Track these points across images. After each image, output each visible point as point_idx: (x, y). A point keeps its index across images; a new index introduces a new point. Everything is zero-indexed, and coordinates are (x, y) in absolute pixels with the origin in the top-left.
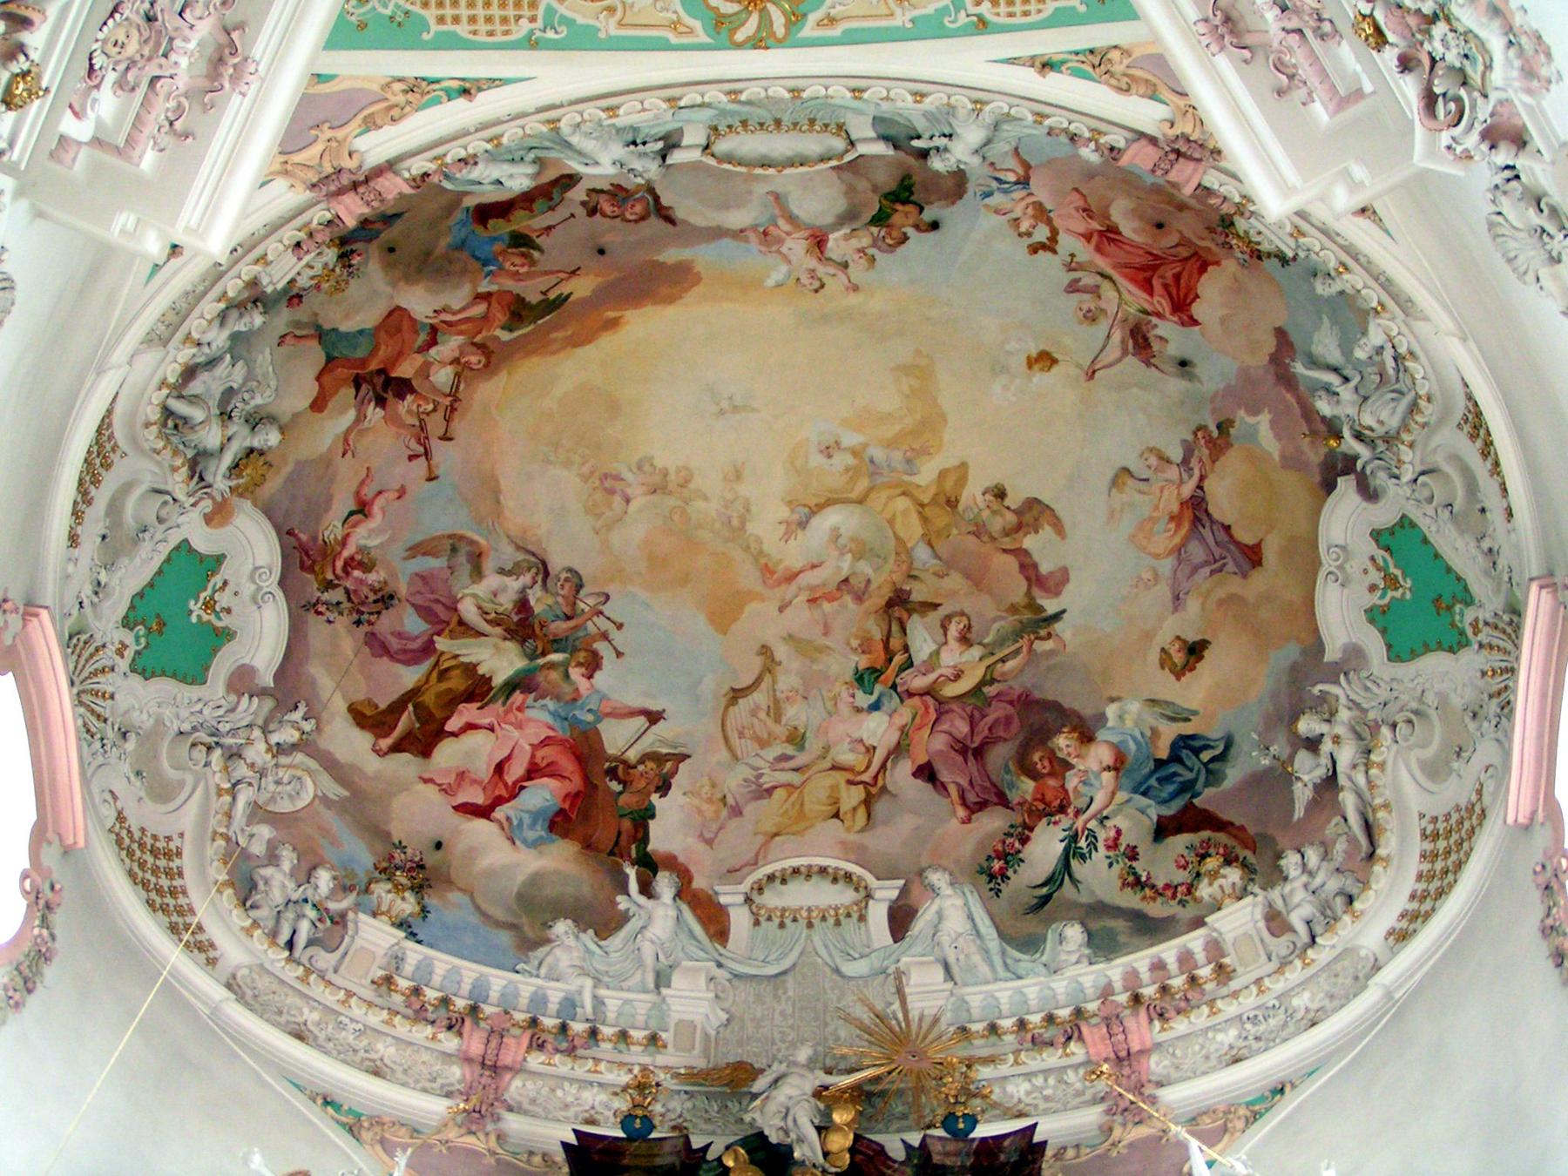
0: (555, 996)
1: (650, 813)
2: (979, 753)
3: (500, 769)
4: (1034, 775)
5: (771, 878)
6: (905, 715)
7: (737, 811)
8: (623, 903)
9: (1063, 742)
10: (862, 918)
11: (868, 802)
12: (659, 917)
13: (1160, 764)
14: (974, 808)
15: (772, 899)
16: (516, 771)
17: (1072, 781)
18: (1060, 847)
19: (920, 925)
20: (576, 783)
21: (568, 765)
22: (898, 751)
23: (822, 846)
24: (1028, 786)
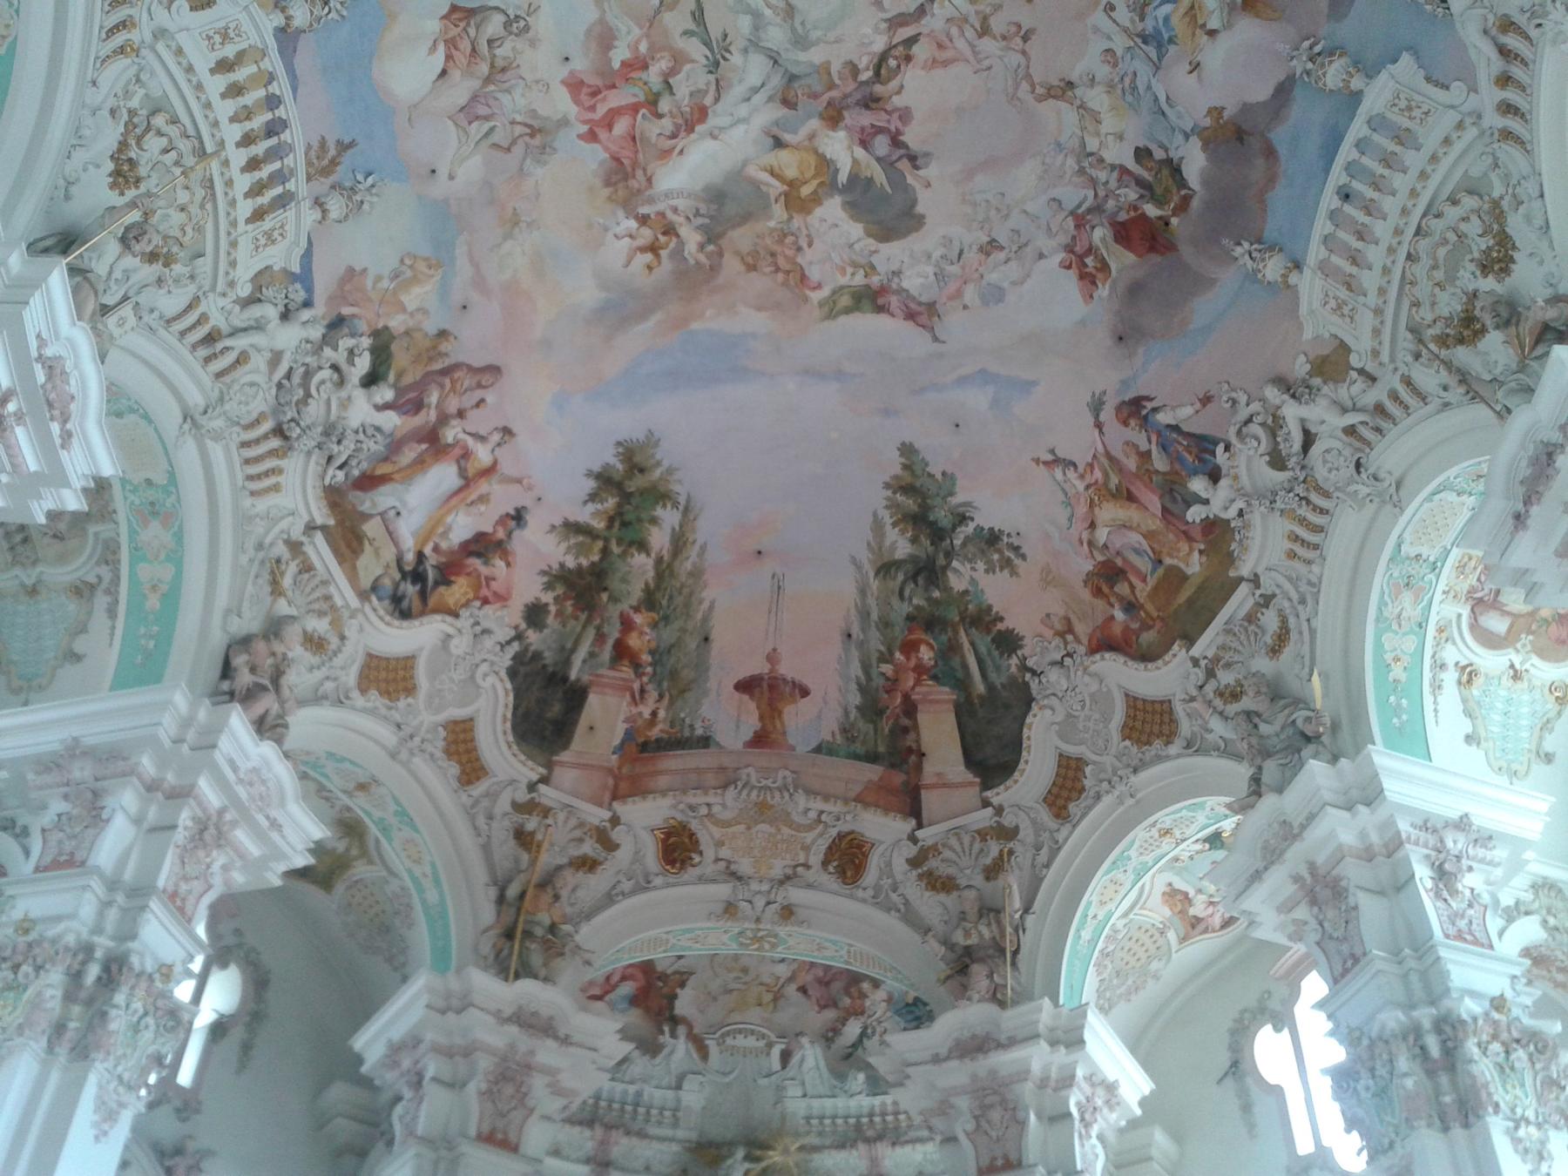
0: (632, 1089)
1: (675, 996)
2: (827, 984)
3: (608, 978)
4: (851, 997)
5: (728, 1034)
6: (795, 966)
7: (715, 999)
8: (661, 1039)
9: (865, 986)
10: (768, 1054)
11: (775, 1000)
12: (679, 1050)
13: (908, 1005)
14: (823, 1007)
15: (729, 1041)
16: (616, 978)
17: (868, 1003)
18: (858, 1031)
19: (795, 1060)
20: (642, 982)
21: (640, 976)
22: (791, 979)
23: (754, 1015)
24: (847, 1001)
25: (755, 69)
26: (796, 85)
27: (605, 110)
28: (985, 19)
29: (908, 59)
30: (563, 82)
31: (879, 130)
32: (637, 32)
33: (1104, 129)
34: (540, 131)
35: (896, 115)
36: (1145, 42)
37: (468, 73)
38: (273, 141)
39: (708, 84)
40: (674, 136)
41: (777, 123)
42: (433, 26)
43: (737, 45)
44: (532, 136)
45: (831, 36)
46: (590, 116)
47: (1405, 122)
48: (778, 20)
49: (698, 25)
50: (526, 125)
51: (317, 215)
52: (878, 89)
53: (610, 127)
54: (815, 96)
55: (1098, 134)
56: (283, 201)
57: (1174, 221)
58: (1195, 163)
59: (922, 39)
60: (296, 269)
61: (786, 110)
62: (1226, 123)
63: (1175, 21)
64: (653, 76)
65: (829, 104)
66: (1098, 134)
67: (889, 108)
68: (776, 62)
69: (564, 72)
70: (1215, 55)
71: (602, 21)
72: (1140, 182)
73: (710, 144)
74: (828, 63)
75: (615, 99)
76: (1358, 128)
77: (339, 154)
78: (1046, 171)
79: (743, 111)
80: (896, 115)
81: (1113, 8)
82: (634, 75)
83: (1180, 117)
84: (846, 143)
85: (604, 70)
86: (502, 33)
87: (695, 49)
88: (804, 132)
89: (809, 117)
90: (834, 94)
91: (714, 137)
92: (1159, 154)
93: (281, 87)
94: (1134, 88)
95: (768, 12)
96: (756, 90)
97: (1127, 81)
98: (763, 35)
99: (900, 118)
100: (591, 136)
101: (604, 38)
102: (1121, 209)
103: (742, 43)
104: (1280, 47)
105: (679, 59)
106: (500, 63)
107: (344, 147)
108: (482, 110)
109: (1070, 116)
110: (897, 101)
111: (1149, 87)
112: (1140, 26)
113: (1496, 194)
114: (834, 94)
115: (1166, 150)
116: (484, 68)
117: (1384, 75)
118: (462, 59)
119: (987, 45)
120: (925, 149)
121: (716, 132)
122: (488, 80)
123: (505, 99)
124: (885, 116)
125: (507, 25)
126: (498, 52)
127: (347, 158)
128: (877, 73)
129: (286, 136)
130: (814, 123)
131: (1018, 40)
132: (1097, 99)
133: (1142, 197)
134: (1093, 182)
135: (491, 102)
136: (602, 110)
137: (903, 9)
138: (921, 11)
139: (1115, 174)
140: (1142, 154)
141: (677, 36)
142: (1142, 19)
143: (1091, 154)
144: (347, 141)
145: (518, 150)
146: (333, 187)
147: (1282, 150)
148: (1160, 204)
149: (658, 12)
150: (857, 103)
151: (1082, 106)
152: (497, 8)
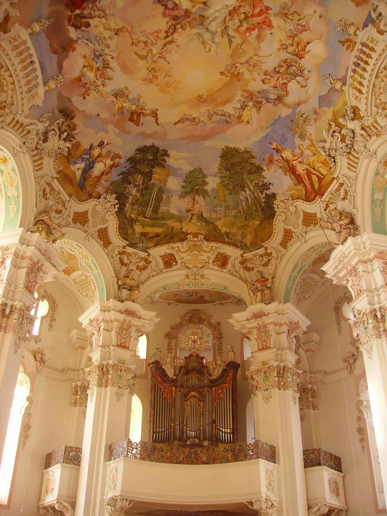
25: (213, 27)
26: (200, 22)
27: (262, 17)
28: (146, 46)
29: (166, 32)
30: (273, 27)
31: (172, 9)
32: (249, 39)
33: (102, 26)
34: (284, 14)
35: (167, 15)
36: (100, 55)
37: (301, 40)
38: (359, 62)
39: (228, 22)
40: (240, 6)
41: (206, 10)
42: (307, 57)
43: (219, 34)
44: (287, 14)
45: (190, 37)
46: (267, 15)
47: (31, 93)
48: (207, 40)
49: (231, 40)
50: (288, 18)
51: (358, 32)
52: (174, 23)
53: (261, 11)
54: (194, 19)
55: (103, 24)
56: (364, 45)
57: (70, 13)
58: (73, 33)
59: (163, 38)
60: (370, 25)
61: (203, 14)
62: (69, 51)
63: (95, 64)
64: (245, 26)
65: (189, 17)
66: (103, 24)
67: (170, 17)
68: (207, 29)
69: (273, 30)
70: (81, 62)
71: (259, 42)
72: (85, 17)
73: (228, 3)
74: (191, 29)
75: (258, 19)
76: (40, 80)
77: (345, 42)
78: (115, 6)
79: (217, 14)
80: (167, 15)
81: (112, 58)
82: (252, 26)
83: (82, 42)
84: (182, 5)
85: (260, 29)
86: (289, 46)
87: (232, 33)
88: (197, 7)
89: (195, 12)
90: (188, 20)
91: (227, 6)
92: (84, 28)
93: (350, 73)
94: (98, 42)
95: (210, 42)
96: (213, 20)
97: (101, 42)
98: (211, 36)
99: (166, 14)
100: (267, 8)
101: (259, 38)
102: (87, 6)
103: (218, 34)
104: (67, 76)
105: (237, 30)
106: (291, 39)
107: (343, 43)
108: (300, 27)
109: (113, 25)
110: (167, 19)
111: (94, 45)
112: (103, 57)
113: (6, 109)
114: (188, 20)
115: (82, 31)
116: (296, 39)
117: (43, 98)
118: (302, 45)
119: (144, 39)
120: (156, 5)
121: (226, 7)
122: (296, 35)
123: (292, 28)
124: (170, 14)
125: (287, 48)
126: (291, 42)
127: (343, 39)
128: (175, 27)
129: (355, 60)
130: (193, 11)
131: (135, 42)
132: (107, 34)
133: (82, 13)
134: (99, 9)
135: (296, 29)
136: (263, 17)
137: (170, 45)
138: (165, 45)
139: (93, 15)
140: (88, 25)
141: (237, 36)
142: (103, 59)
143: (102, 17)
144: (341, 44)
145: (292, 11)
146: (350, 35)
147: (53, 55)
148: (77, 15)
149: (242, 43)
150: (180, 18)
151: (110, 30)
152: (288, 53)
